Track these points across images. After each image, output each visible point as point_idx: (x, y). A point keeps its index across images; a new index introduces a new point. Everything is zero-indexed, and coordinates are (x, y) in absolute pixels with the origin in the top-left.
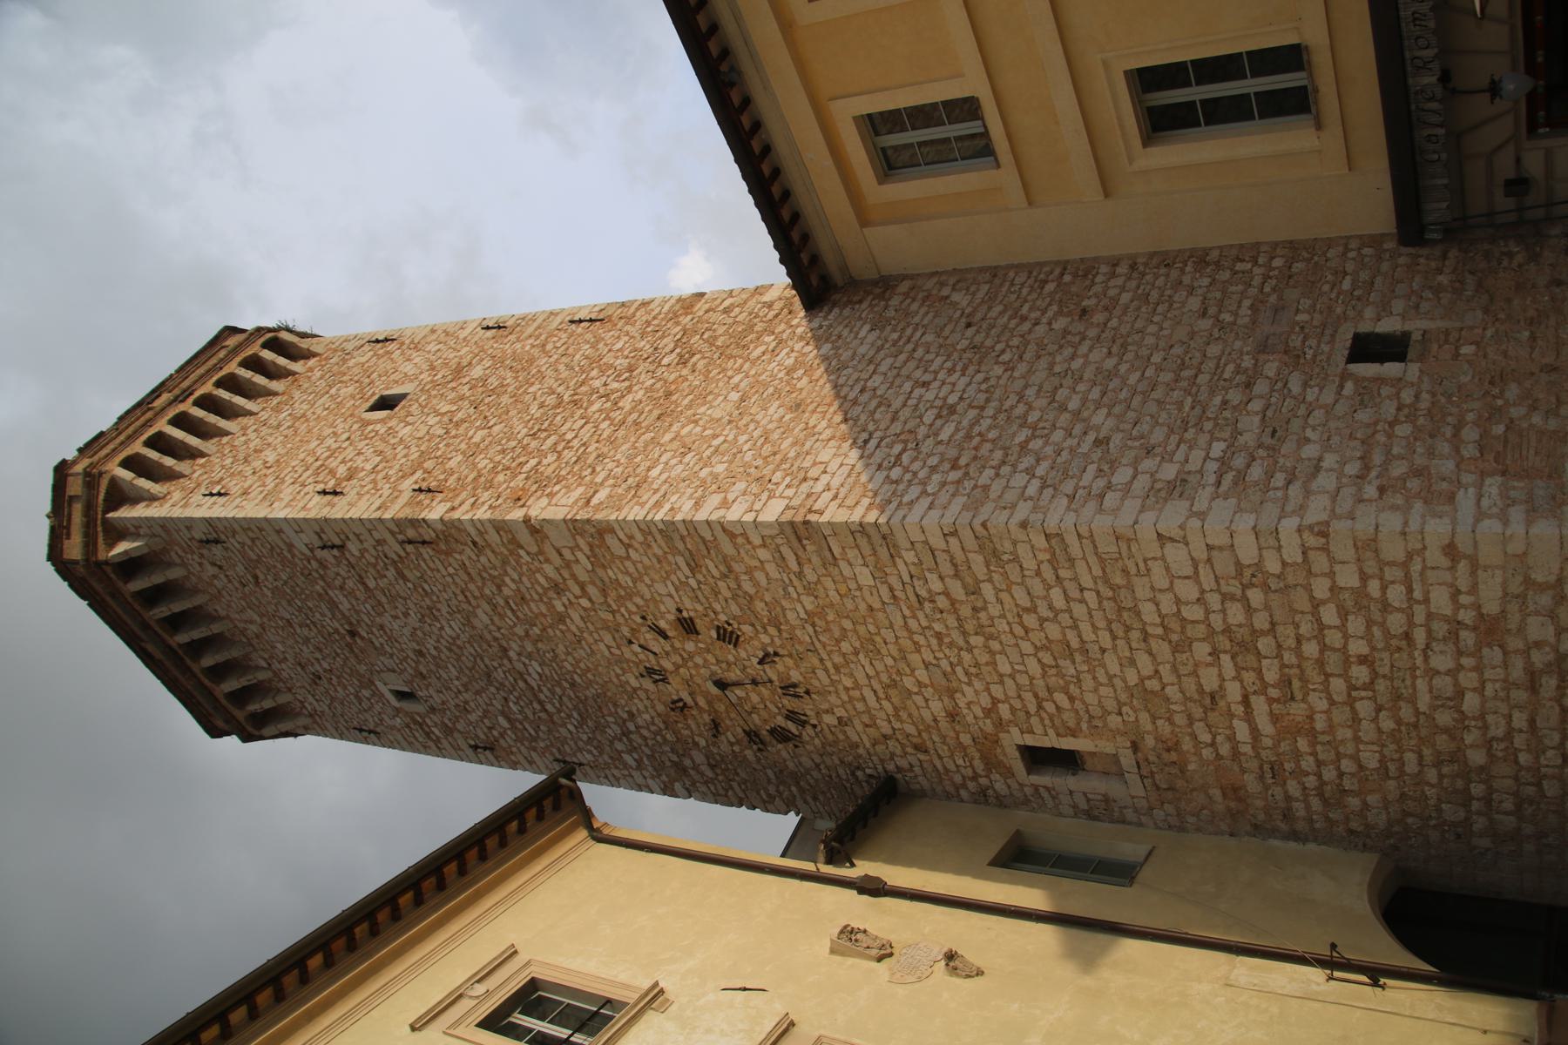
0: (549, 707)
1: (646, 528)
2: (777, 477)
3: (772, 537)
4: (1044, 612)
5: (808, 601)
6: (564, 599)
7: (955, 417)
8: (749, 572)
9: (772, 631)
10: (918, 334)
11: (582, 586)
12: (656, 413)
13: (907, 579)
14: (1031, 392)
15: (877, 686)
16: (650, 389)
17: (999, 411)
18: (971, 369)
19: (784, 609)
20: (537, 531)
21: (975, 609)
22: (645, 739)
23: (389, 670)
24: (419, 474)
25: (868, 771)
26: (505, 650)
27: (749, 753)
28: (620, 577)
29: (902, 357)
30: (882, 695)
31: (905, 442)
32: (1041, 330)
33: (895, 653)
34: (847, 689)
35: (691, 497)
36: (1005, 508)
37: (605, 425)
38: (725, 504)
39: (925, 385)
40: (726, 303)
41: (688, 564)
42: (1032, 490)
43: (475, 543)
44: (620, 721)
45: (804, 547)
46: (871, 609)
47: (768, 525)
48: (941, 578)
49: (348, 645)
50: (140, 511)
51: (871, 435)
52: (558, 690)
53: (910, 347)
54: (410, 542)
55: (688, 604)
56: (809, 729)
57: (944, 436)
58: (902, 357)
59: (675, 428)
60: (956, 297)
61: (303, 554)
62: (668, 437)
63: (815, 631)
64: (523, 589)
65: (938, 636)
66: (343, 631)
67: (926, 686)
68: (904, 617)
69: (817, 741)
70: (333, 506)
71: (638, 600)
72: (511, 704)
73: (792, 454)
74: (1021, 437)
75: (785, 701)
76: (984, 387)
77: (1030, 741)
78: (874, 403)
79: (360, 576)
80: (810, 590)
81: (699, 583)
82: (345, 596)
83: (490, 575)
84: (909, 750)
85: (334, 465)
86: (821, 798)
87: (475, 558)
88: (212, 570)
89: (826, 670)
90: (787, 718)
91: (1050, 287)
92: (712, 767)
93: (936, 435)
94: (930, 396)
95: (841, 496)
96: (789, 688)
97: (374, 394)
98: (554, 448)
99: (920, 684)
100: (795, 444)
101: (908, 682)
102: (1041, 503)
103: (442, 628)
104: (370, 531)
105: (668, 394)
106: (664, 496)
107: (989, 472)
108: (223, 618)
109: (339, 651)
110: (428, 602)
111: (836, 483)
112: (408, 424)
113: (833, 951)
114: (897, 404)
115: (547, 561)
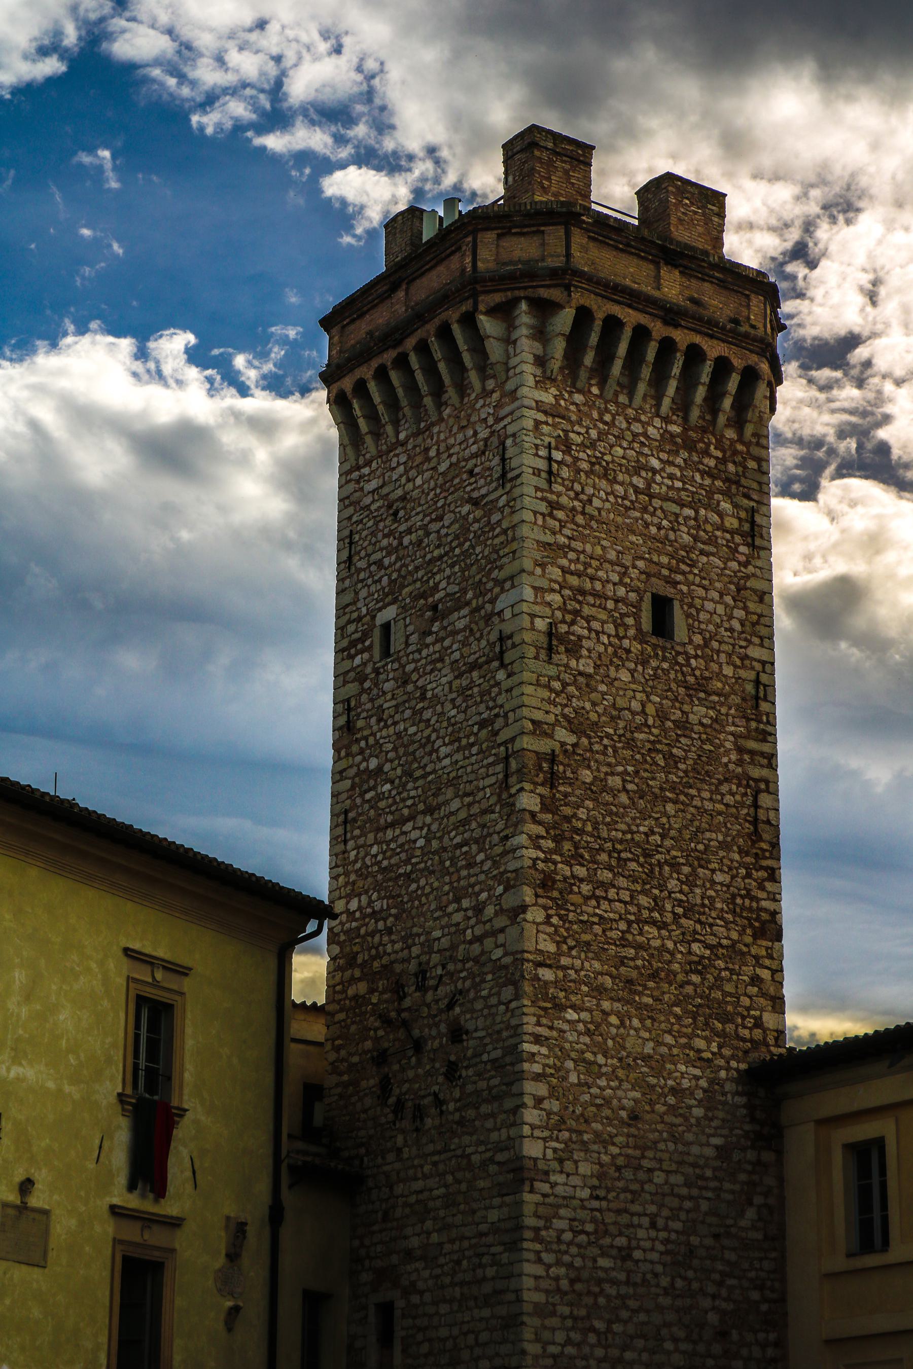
0: (390, 834)
1: (517, 1031)
2: (565, 1135)
3: (514, 1147)
4: (478, 1351)
5: (476, 1158)
6: (470, 913)
7: (619, 1263)
8: (492, 1115)
9: (457, 1116)
10: (710, 1194)
11: (479, 939)
12: (634, 974)
13: (494, 1250)
14: (642, 1317)
15: (426, 1194)
16: (663, 948)
17: (623, 1297)
18: (668, 1259)
19: (471, 1134)
20: (516, 916)
21: (476, 1298)
22: (372, 934)
23: (408, 637)
24: (572, 739)
25: (366, 1159)
26: (430, 810)
27: (368, 1044)
28: (488, 985)
29: (684, 1191)
30: (421, 1197)
31: (596, 1232)
32: (707, 1303)
33: (449, 1220)
34: (422, 1166)
35: (545, 1066)
36: (536, 1334)
37: (623, 926)
38: (539, 1101)
39: (653, 1225)
40: (765, 974)
41: (496, 1060)
42: (553, 1349)
43: (507, 838)
44: (384, 914)
45: (508, 1172)
46: (474, 1212)
47: (521, 1144)
48: (493, 1278)
49: (423, 595)
50: (527, 347)
51: (605, 1198)
52: (403, 856)
53: (695, 1192)
54: (507, 758)
55: (472, 1043)
56: (391, 1117)
57: (603, 1262)
58: (684, 1191)
59: (618, 1006)
60: (751, 1213)
61: (496, 598)
62: (606, 1005)
63: (457, 1157)
64: (477, 870)
65: (458, 1262)
66: (437, 596)
67: (428, 1238)
68: (469, 1238)
69: (383, 1120)
70: (536, 658)
71: (472, 994)
72: (388, 787)
73: (586, 1137)
74: (599, 1325)
75: (410, 1104)
76: (649, 1276)
77: (398, 1313)
78: (635, 1187)
79: (480, 667)
80: (484, 1164)
81: (486, 1063)
82: (464, 630)
83: (486, 837)
84: (384, 1206)
85: (587, 610)
86: (342, 1103)
87: (498, 828)
88: (483, 434)
89: (433, 1153)
90: (399, 1100)
91: (755, 1295)
92: (356, 997)
93: (603, 1255)
94: (641, 1234)
95: (547, 1200)
96: (419, 1113)
97: (675, 584)
98: (602, 885)
99: (429, 1233)
100: (597, 1134)
101: (429, 1224)
102: (540, 1361)
103: (445, 744)
104: (513, 710)
105: (654, 976)
106: (547, 1039)
107: (566, 1310)
108: (440, 413)
109: (420, 574)
110: (464, 742)
111: (559, 1190)
112: (632, 672)
113: (228, 1218)
114: (636, 1208)
115: (496, 914)
